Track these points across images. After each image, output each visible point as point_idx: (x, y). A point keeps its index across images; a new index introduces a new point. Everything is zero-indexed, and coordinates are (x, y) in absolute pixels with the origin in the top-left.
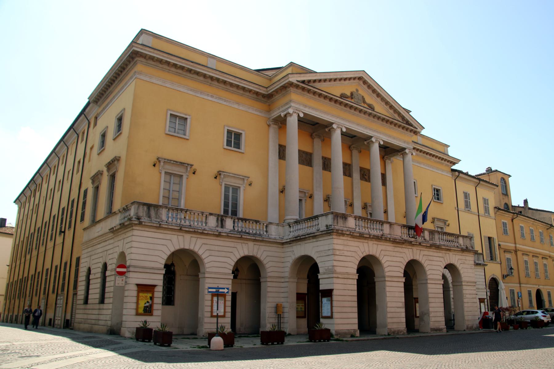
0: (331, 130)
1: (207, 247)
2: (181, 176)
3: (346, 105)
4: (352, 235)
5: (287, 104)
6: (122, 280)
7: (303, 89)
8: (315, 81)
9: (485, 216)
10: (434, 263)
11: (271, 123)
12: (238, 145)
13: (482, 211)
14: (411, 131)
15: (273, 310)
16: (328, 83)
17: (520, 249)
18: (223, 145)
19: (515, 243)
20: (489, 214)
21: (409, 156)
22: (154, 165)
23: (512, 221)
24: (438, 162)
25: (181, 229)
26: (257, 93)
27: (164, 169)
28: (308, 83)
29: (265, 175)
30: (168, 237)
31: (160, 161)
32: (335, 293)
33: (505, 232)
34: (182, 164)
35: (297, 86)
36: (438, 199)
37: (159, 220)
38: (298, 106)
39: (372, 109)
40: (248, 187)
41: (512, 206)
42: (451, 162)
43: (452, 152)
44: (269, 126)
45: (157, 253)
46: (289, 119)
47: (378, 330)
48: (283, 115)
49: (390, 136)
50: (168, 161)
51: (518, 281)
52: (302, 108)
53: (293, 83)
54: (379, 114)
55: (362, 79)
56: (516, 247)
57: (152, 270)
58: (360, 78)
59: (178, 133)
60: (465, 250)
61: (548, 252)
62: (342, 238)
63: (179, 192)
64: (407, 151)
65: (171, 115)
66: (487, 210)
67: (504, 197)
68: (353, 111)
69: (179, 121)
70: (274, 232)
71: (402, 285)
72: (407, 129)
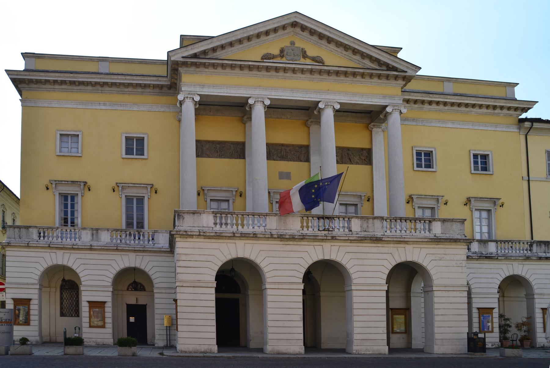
8: (214, 50)
16: (237, 47)
35: (185, 64)
38: (196, 85)
49: (354, 94)
53: (177, 61)
64: (388, 109)
68: (281, 74)
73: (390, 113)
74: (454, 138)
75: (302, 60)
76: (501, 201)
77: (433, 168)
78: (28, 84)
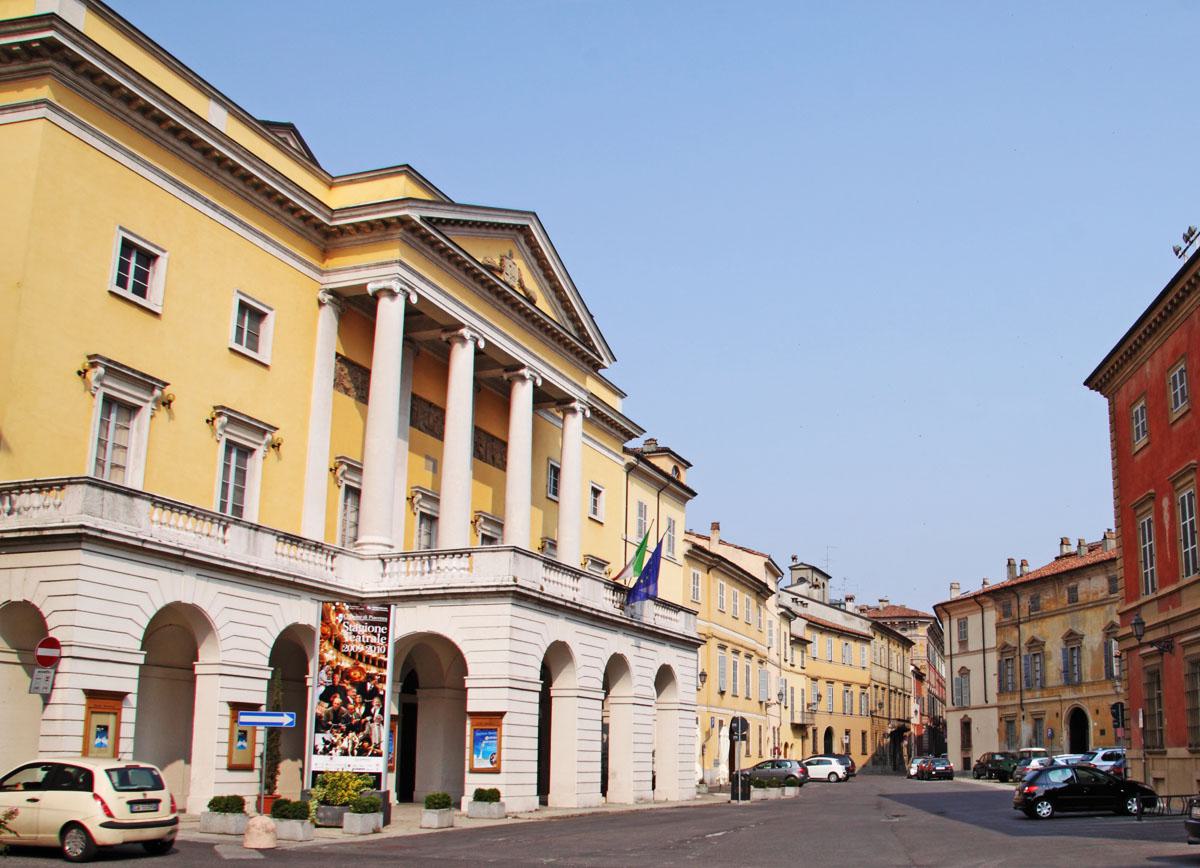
11: (327, 298)
20: (673, 553)
27: (103, 385)
39: (532, 301)
44: (321, 304)
45: (126, 611)
46: (384, 303)
48: (371, 288)
53: (413, 220)
58: (524, 230)
61: (754, 642)
64: (576, 405)
69: (138, 260)
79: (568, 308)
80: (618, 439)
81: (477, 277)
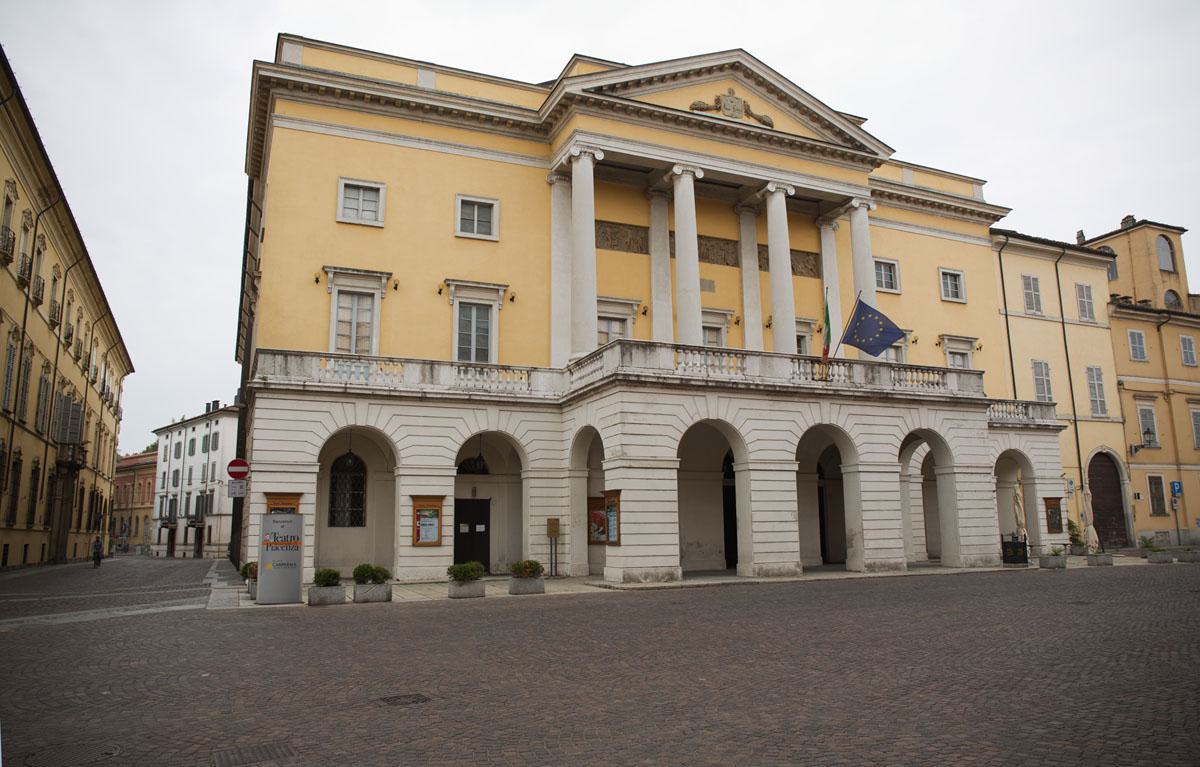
0: (674, 178)
1: (404, 420)
2: (372, 295)
3: (700, 125)
4: (664, 385)
5: (571, 137)
6: (241, 487)
7: (598, 104)
8: (625, 86)
9: (1081, 324)
10: (875, 429)
11: (554, 178)
12: (486, 226)
13: (1072, 312)
14: (863, 160)
15: (544, 530)
17: (1177, 389)
18: (455, 231)
19: (1166, 378)
20: (1092, 317)
21: (862, 213)
22: (317, 281)
23: (1159, 330)
24: (954, 218)
25: (345, 394)
26: (517, 124)
27: (336, 285)
28: (610, 92)
29: (557, 275)
30: (325, 406)
31: (326, 273)
32: (623, 496)
33: (1138, 355)
34: (369, 275)
35: (583, 101)
36: (956, 295)
37: (304, 378)
38: (593, 137)
40: (508, 305)
41: (1189, 296)
42: (987, 216)
43: (991, 196)
44: (551, 184)
45: (303, 436)
47: (850, 564)
48: (564, 160)
50: (340, 272)
51: (1172, 458)
52: (600, 141)
53: (575, 95)
54: (790, 137)
55: (738, 67)
56: (1167, 385)
57: (294, 468)
58: (735, 67)
59: (362, 218)
60: (955, 402)
62: (641, 389)
63: (370, 324)
64: (855, 203)
65: (346, 186)
66: (1086, 308)
67: (1166, 278)
70: (545, 387)
71: (793, 476)
72: (853, 158)
73: (856, 209)
74: (923, 249)
75: (745, 118)
76: (978, 342)
77: (896, 289)
78: (291, 90)
79: (817, 119)
80: (981, 224)
81: (687, 122)
